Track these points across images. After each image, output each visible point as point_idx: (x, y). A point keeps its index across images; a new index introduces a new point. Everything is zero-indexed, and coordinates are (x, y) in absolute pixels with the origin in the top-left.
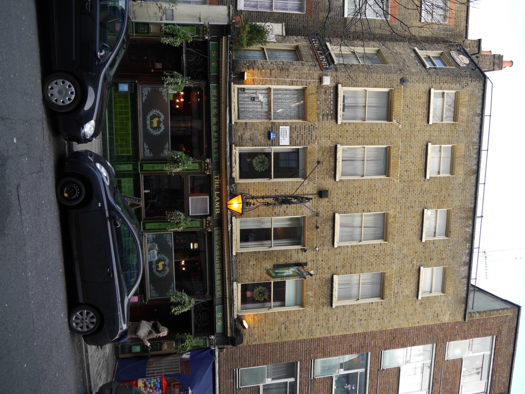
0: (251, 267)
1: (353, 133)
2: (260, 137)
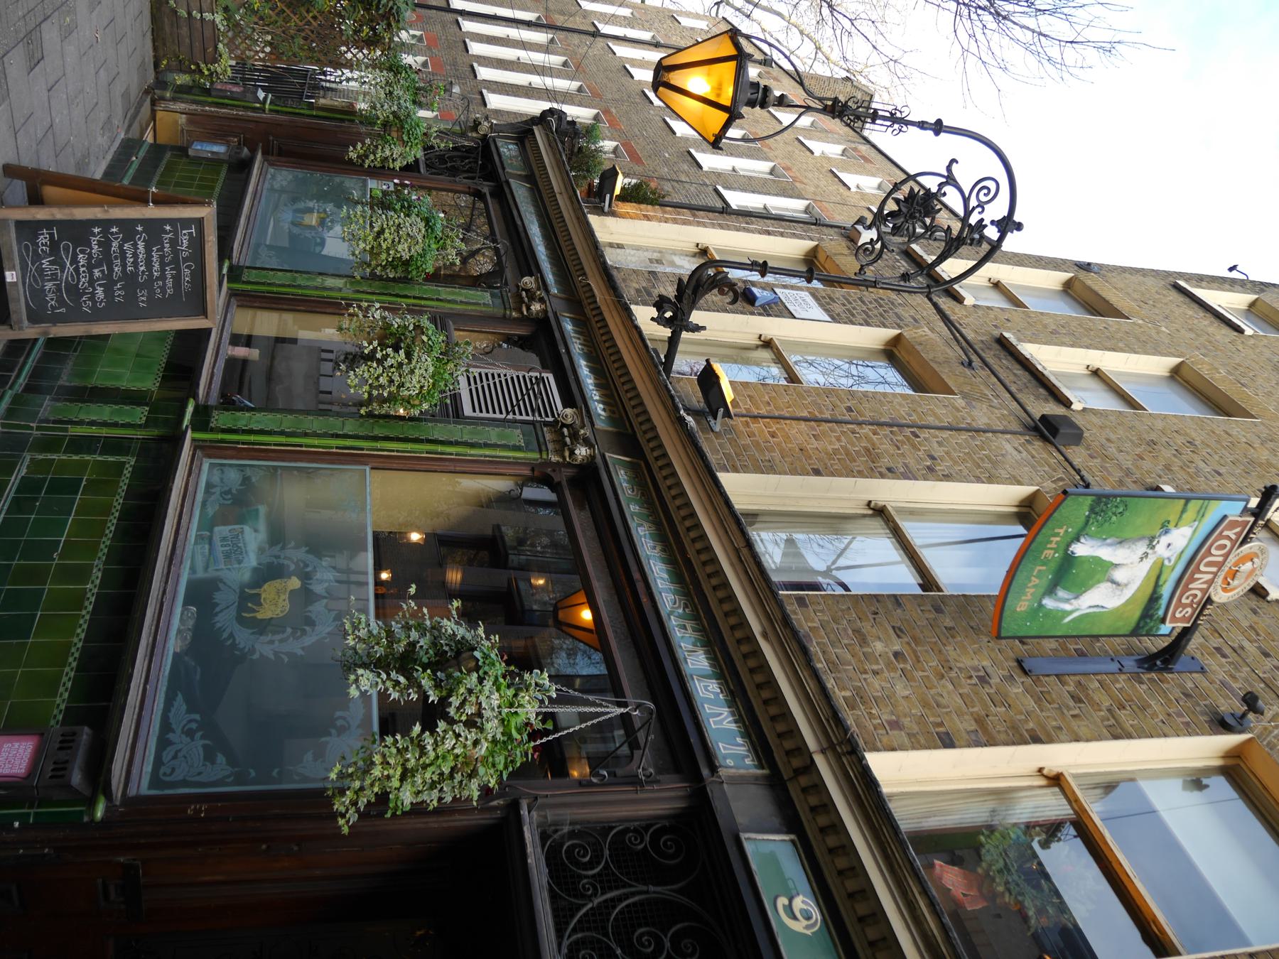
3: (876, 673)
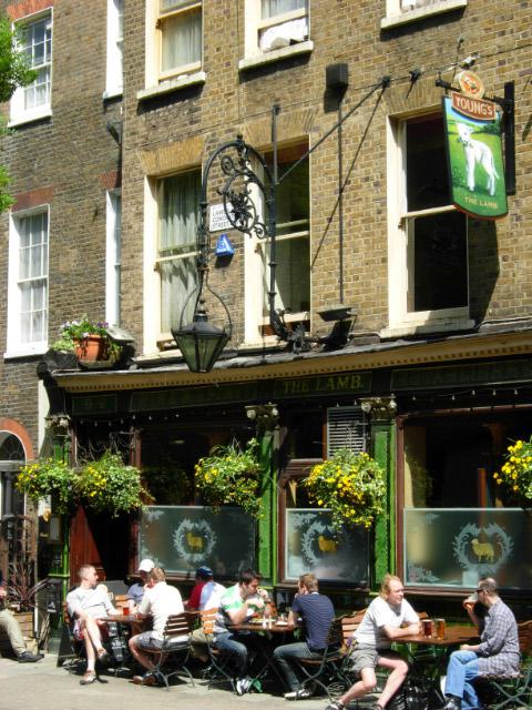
0: (510, 266)
1: (222, 31)
2: (228, 280)
3: (514, 275)
